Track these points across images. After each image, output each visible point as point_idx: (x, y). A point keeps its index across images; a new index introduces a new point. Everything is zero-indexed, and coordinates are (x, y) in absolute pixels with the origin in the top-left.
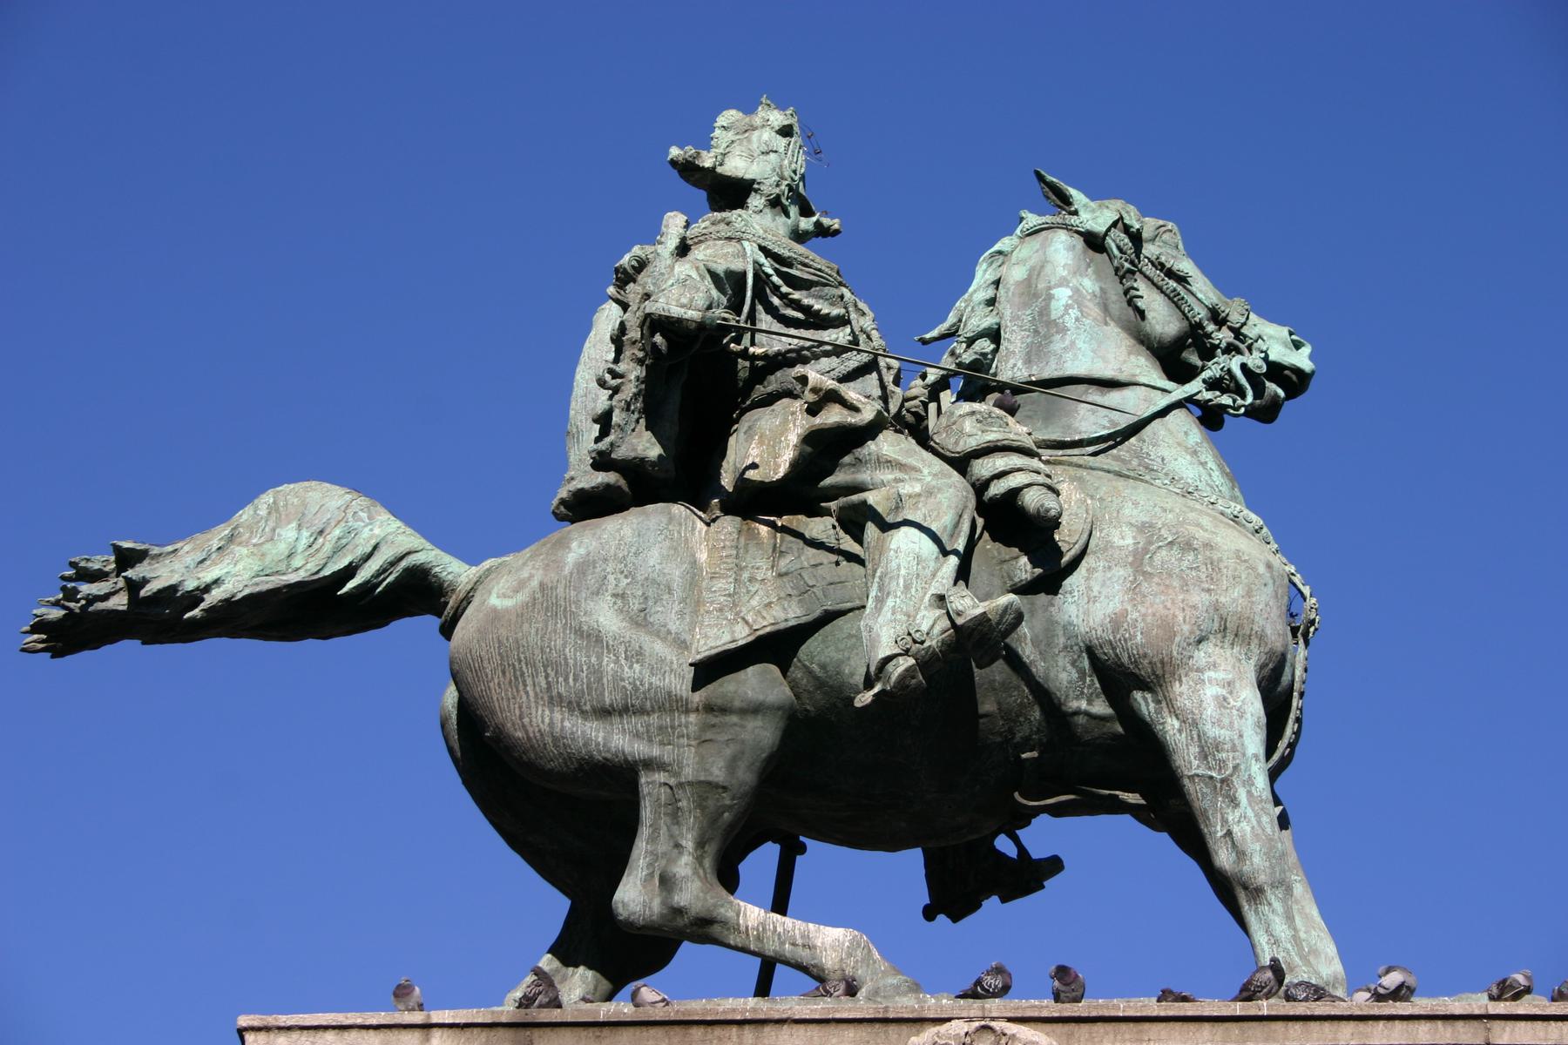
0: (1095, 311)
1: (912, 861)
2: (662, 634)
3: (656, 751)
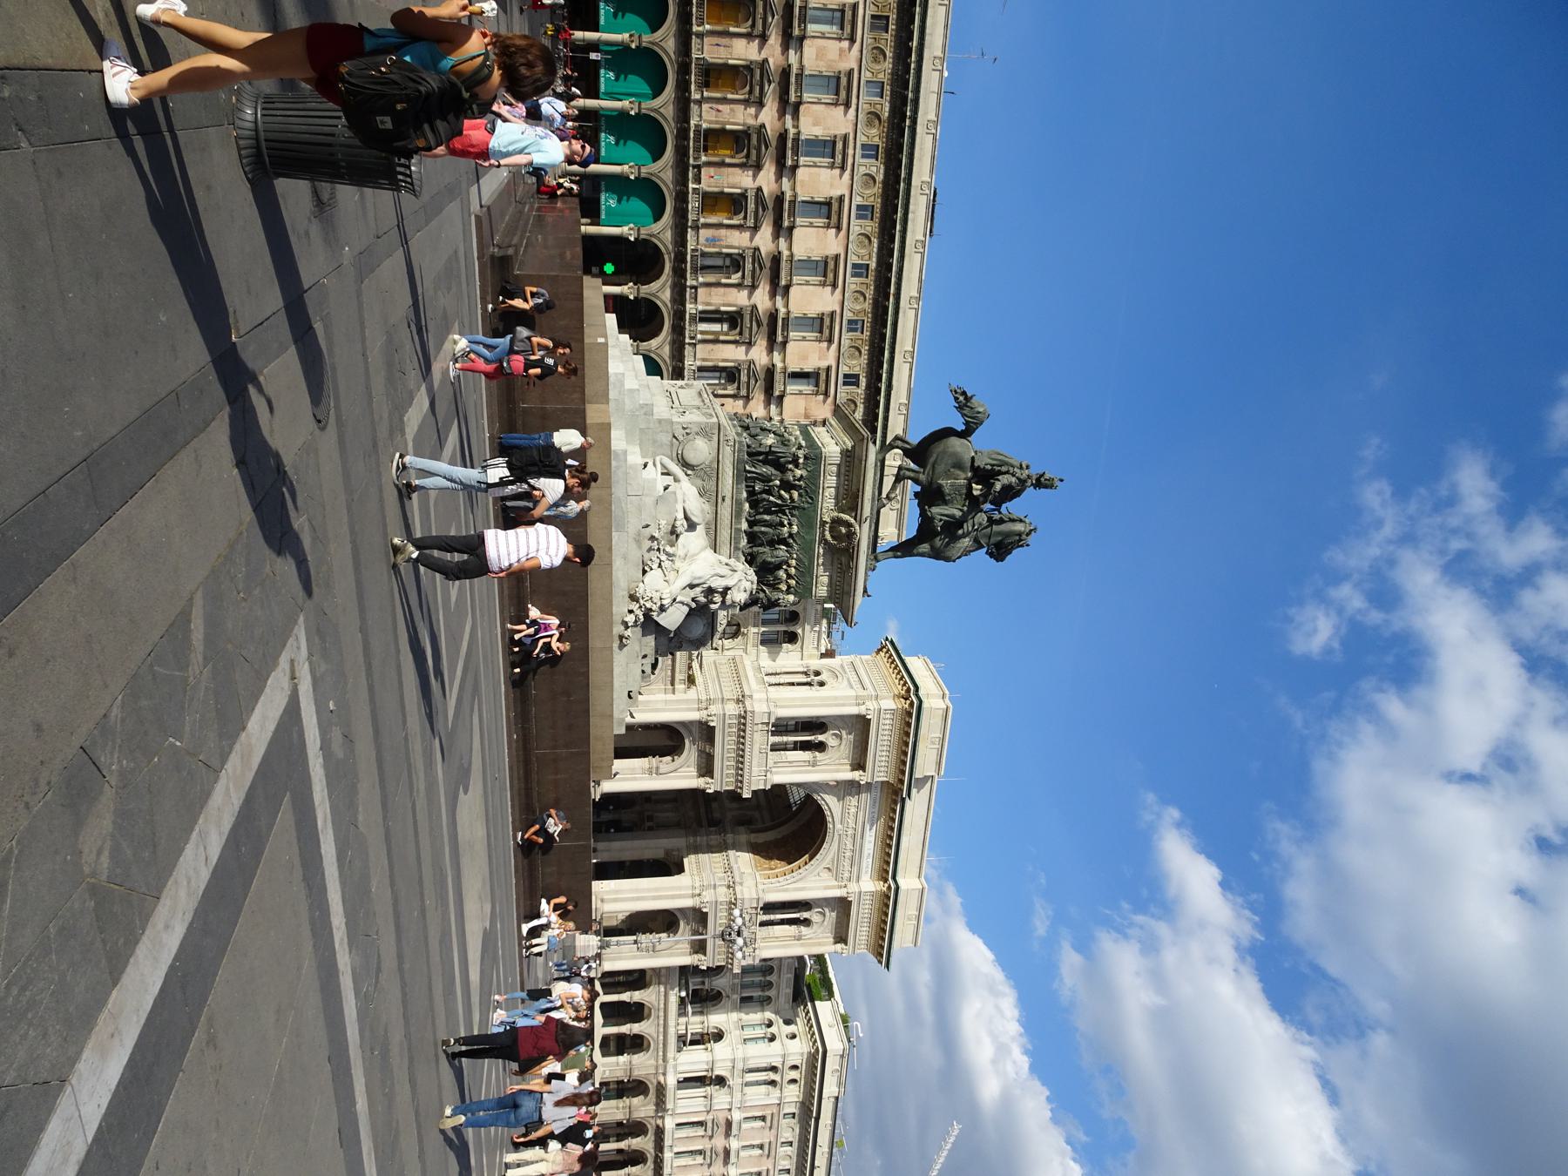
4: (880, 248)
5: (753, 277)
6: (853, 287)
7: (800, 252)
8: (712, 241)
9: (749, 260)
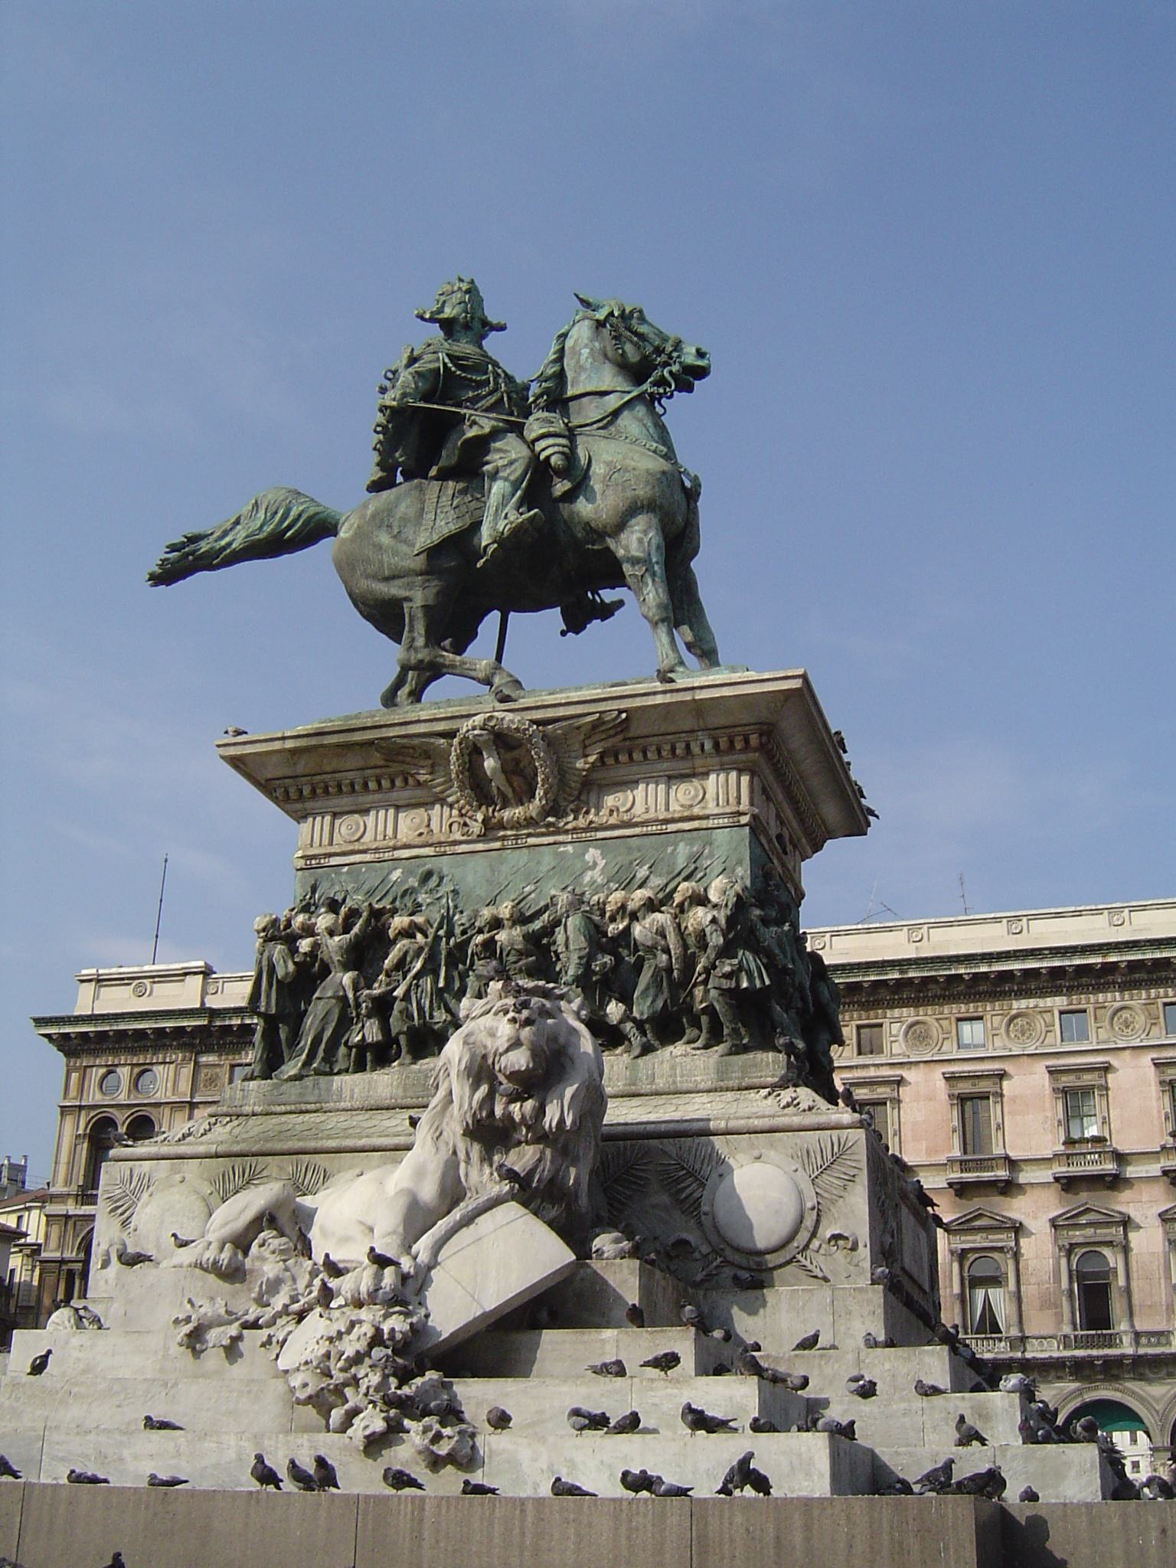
0: (601, 358)
1: (559, 609)
2: (405, 542)
3: (407, 594)
4: (1028, 994)
5: (1108, 1224)
6: (1103, 1034)
7: (1050, 1143)
8: (1048, 1303)
9: (1077, 1236)
